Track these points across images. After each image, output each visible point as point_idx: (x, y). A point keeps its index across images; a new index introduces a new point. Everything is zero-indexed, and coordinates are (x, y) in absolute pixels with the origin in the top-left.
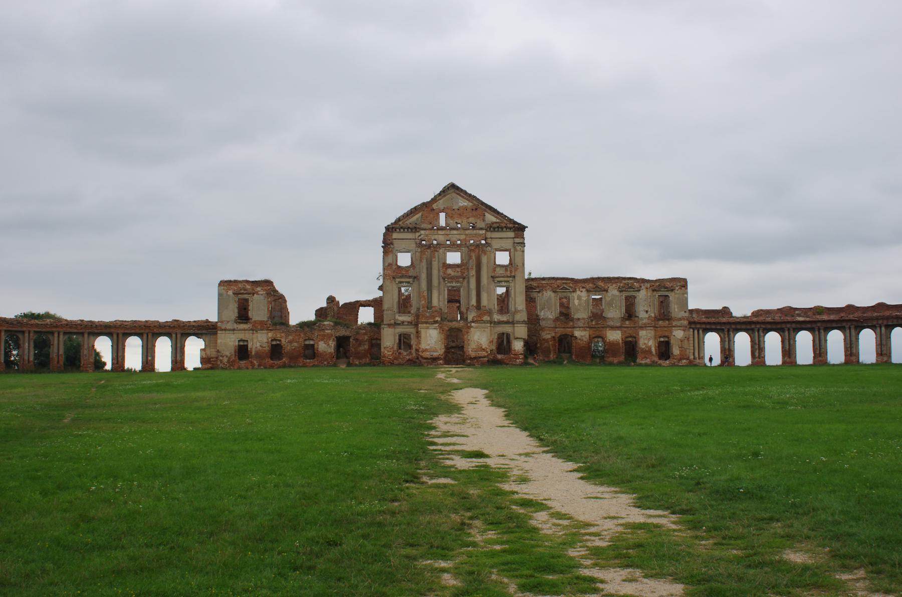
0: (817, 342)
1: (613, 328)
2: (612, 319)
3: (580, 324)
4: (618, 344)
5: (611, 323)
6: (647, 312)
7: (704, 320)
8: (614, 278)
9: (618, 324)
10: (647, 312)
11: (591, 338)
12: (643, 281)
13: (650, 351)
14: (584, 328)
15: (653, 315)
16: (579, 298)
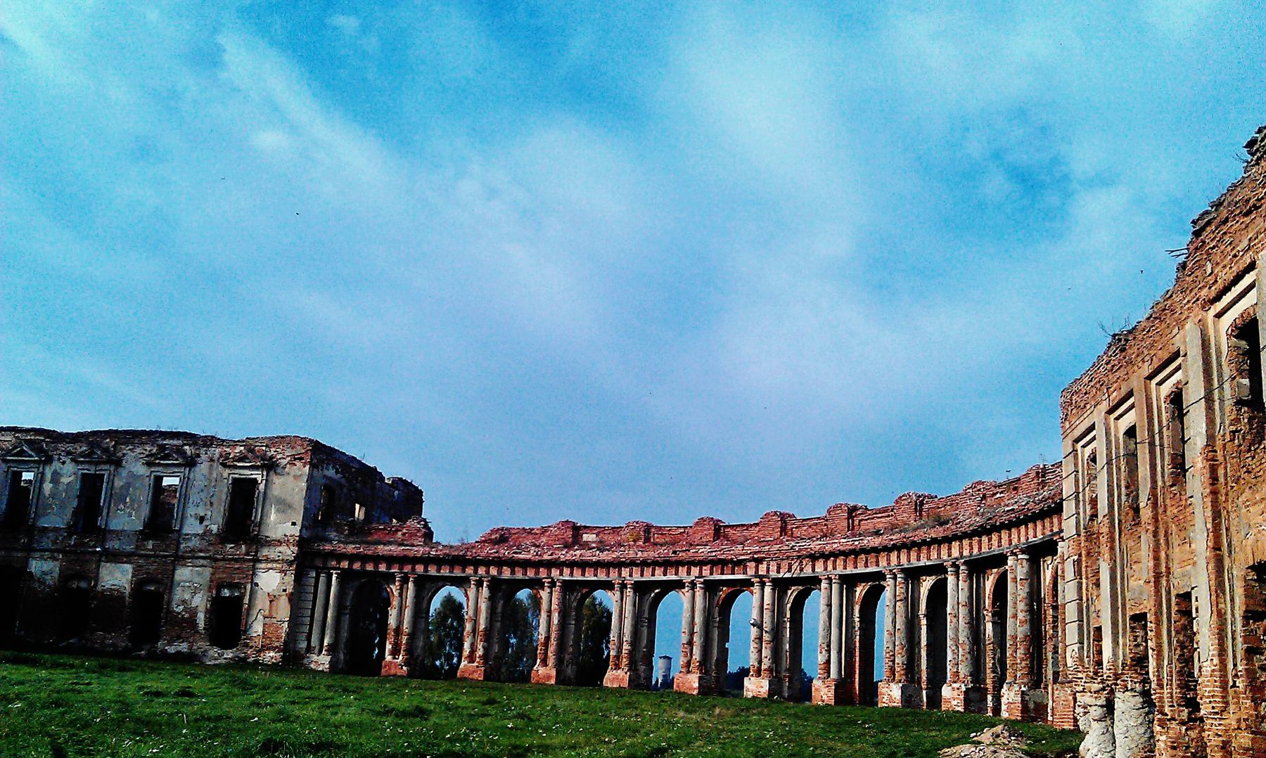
0: (716, 634)
1: (116, 557)
2: (118, 534)
3: (47, 543)
4: (121, 597)
5: (114, 544)
6: (202, 519)
7: (350, 549)
8: (144, 433)
9: (130, 548)
10: (202, 519)
11: (65, 577)
12: (209, 441)
13: (192, 622)
14: (52, 554)
15: (214, 528)
16: (56, 478)
